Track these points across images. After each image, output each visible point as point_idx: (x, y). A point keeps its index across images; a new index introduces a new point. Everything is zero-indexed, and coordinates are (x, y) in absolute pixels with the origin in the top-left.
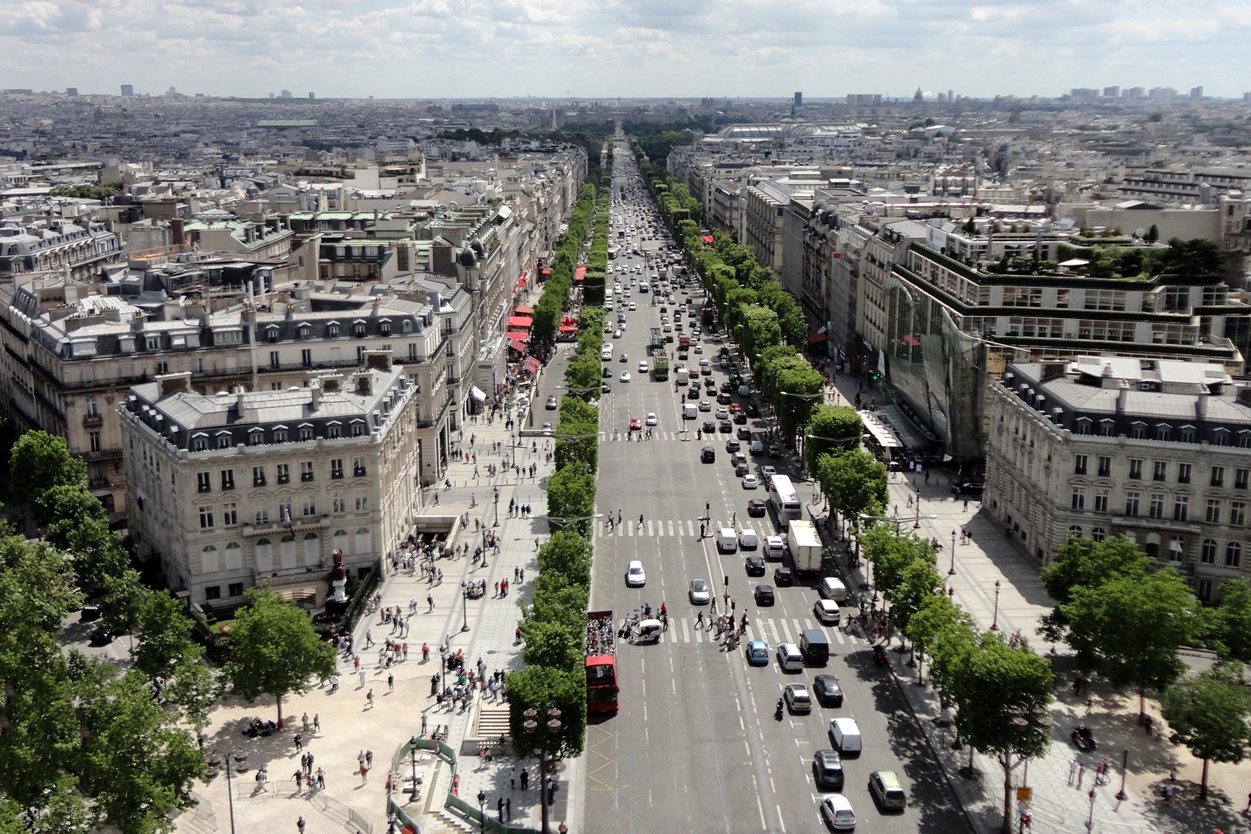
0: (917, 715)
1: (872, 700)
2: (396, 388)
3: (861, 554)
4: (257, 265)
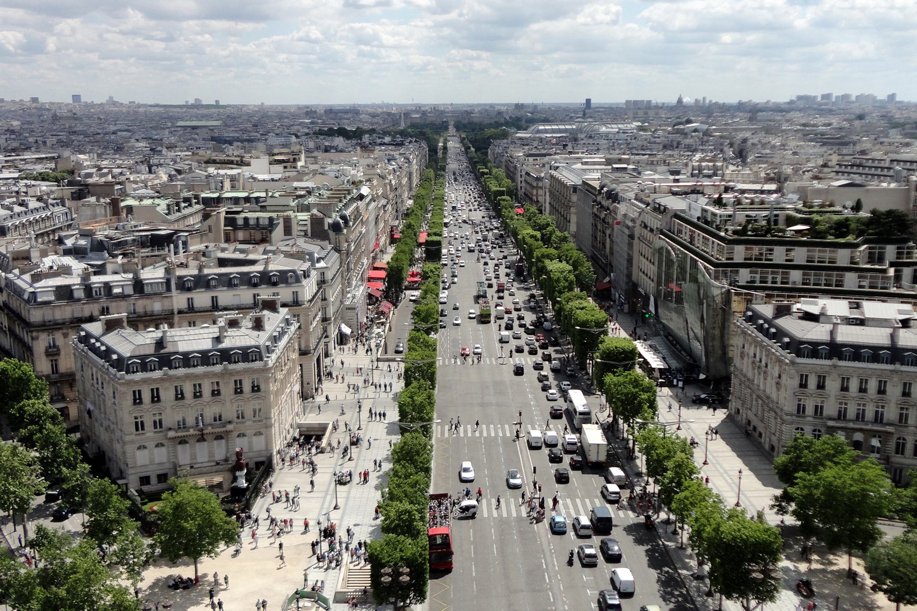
0: (679, 571)
1: (645, 560)
2: (283, 325)
3: (637, 449)
4: (177, 232)
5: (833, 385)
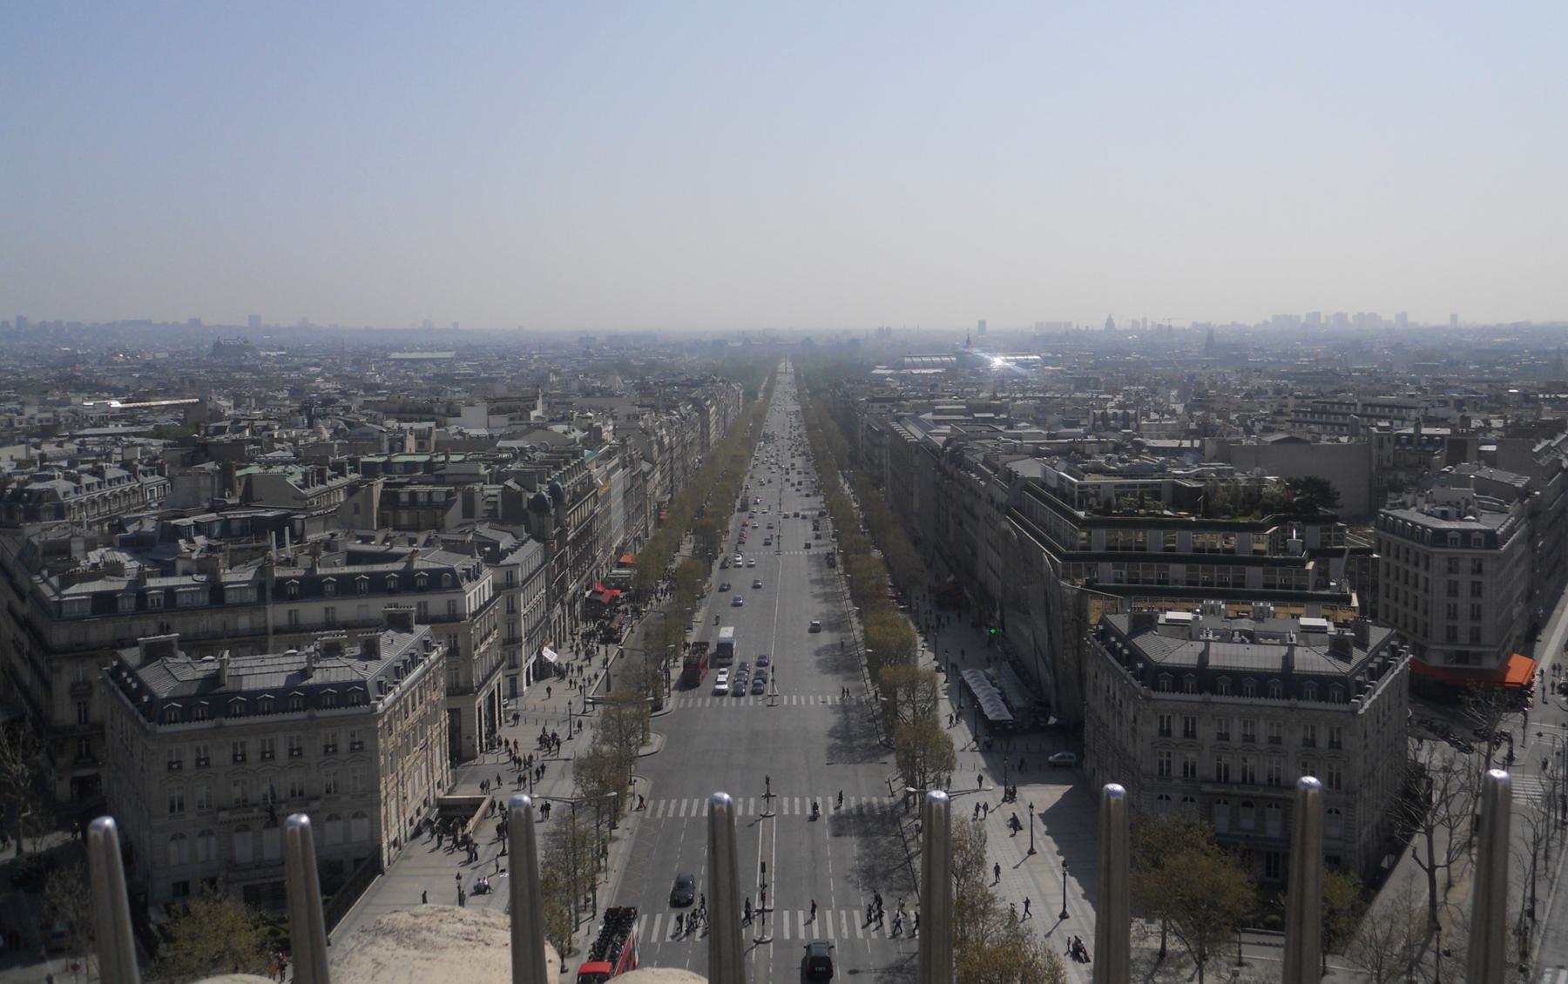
5: (1207, 731)
